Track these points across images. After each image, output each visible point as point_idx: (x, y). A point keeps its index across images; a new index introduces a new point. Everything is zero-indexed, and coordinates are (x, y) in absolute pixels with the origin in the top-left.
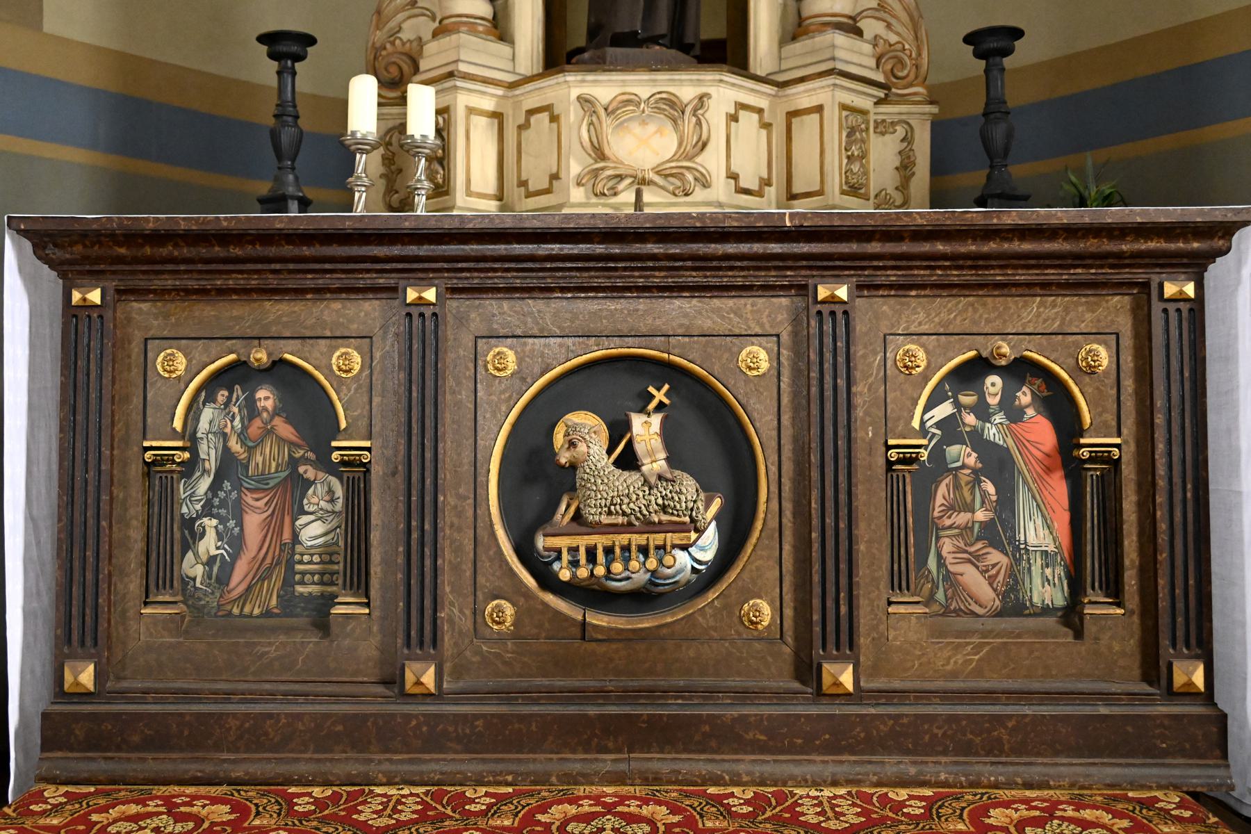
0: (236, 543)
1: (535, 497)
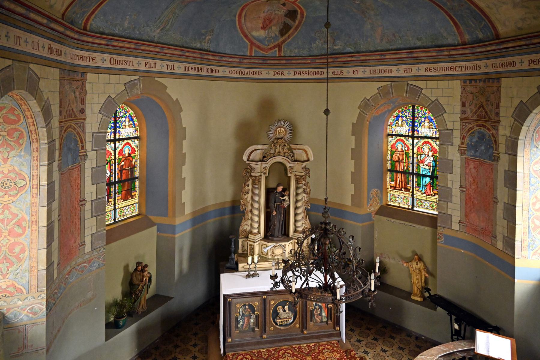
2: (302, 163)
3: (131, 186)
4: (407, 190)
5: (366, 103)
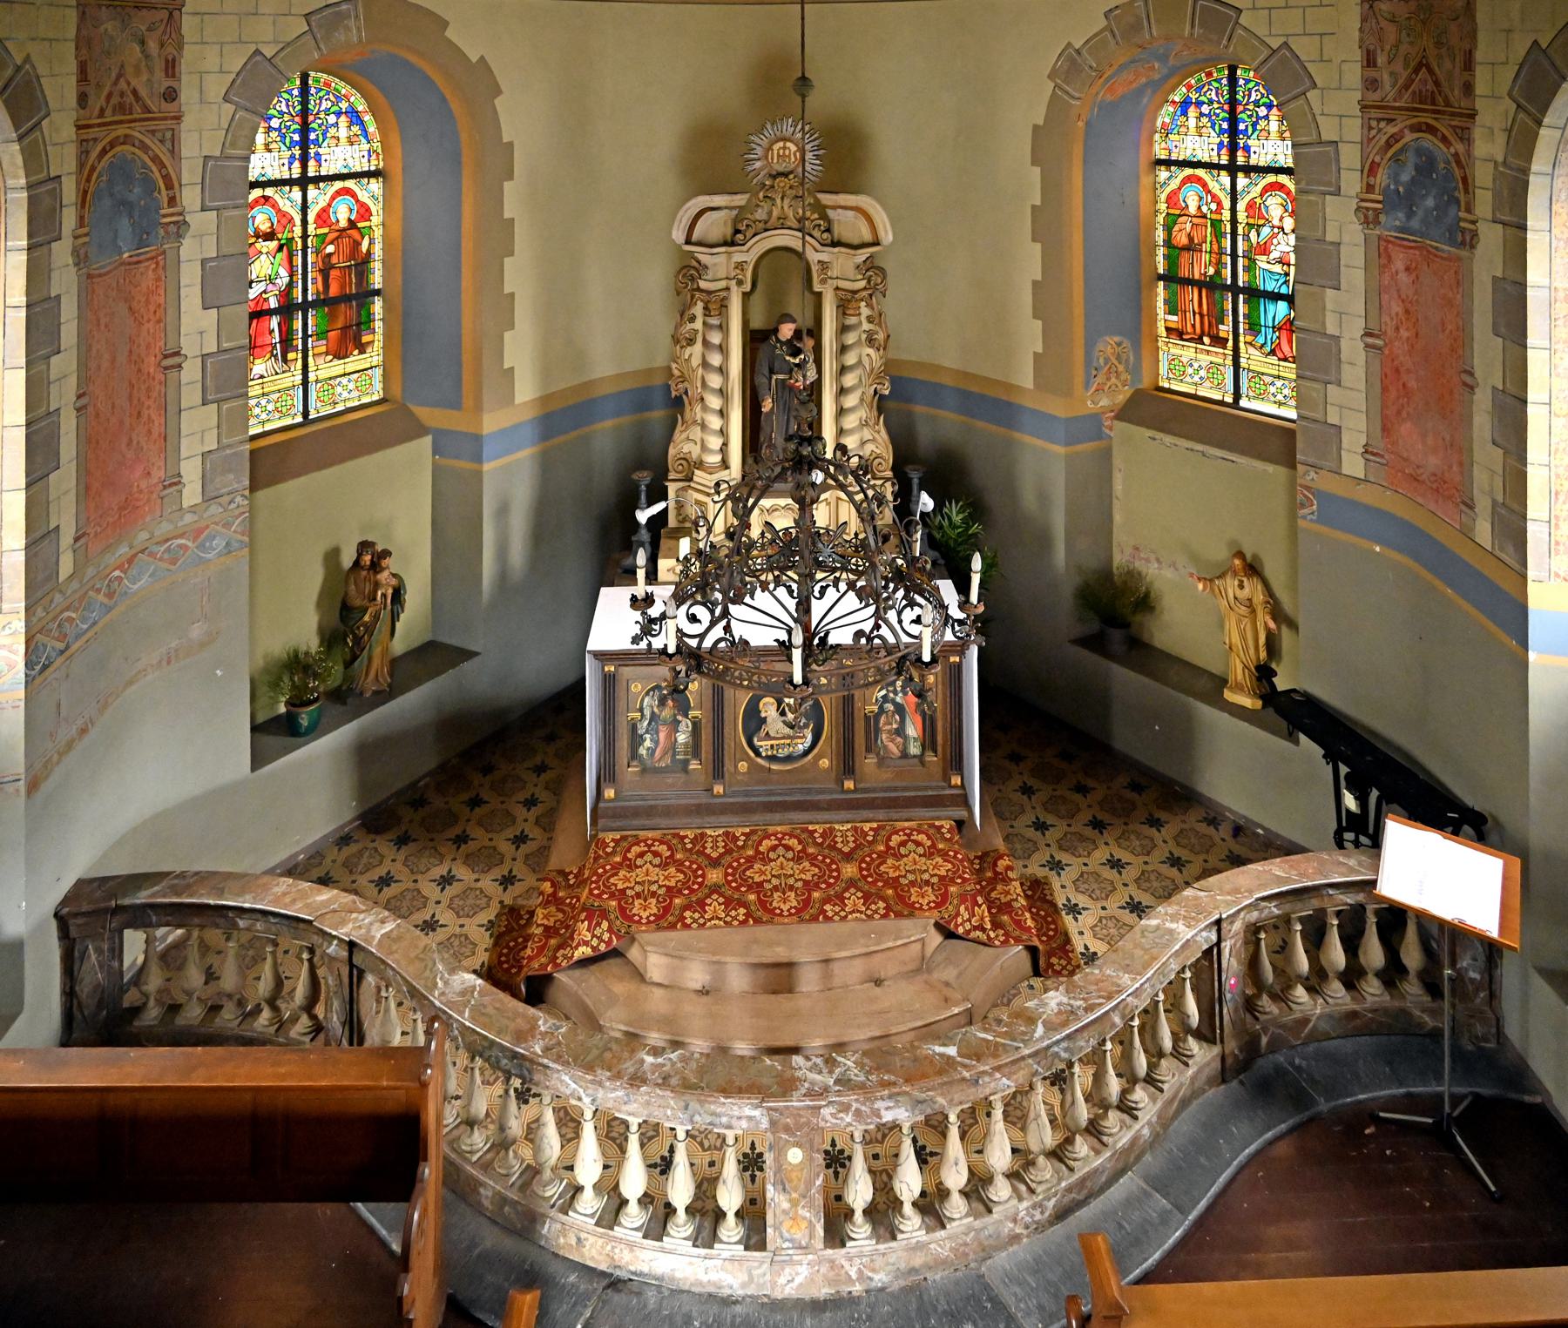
0: (657, 743)
1: (753, 725)
2: (852, 252)
3: (359, 315)
4: (1219, 341)
5: (1073, 61)
